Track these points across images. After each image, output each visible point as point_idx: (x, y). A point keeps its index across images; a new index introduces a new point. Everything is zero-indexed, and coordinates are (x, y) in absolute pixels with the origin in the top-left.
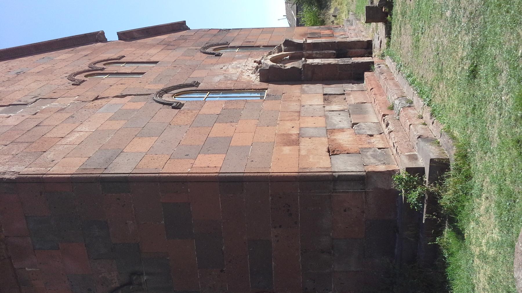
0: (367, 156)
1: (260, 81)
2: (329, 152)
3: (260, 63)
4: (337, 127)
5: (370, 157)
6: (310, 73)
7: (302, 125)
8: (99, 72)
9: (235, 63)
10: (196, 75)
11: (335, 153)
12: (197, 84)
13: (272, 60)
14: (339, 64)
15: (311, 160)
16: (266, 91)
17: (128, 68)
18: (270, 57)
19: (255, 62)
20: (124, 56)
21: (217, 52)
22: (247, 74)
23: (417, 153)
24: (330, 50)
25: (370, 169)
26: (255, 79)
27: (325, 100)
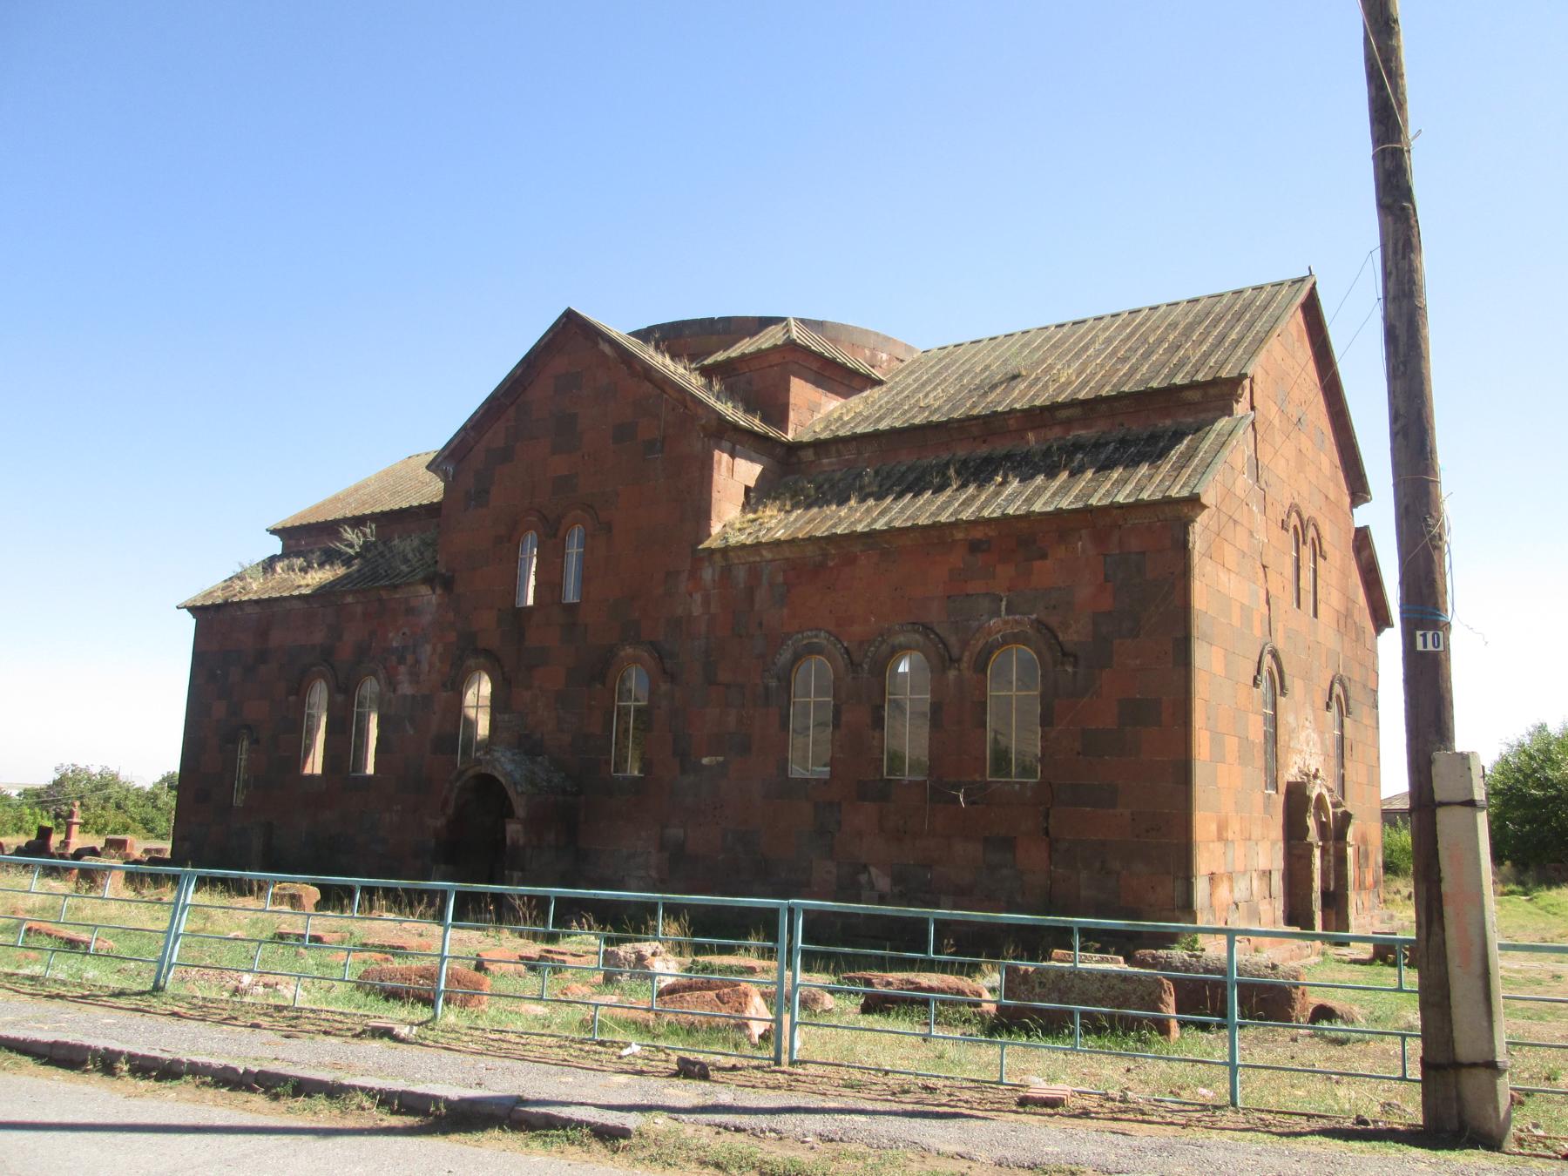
2: (1212, 874)
3: (1315, 777)
4: (1234, 885)
7: (1236, 843)
8: (1301, 539)
9: (1314, 736)
10: (1295, 684)
12: (1283, 694)
13: (1320, 797)
16: (1274, 792)
17: (1306, 576)
18: (1325, 791)
19: (1317, 770)
20: (1325, 559)
21: (1334, 704)
22: (1298, 760)
24: (1335, 883)
26: (1291, 774)
27: (1264, 872)
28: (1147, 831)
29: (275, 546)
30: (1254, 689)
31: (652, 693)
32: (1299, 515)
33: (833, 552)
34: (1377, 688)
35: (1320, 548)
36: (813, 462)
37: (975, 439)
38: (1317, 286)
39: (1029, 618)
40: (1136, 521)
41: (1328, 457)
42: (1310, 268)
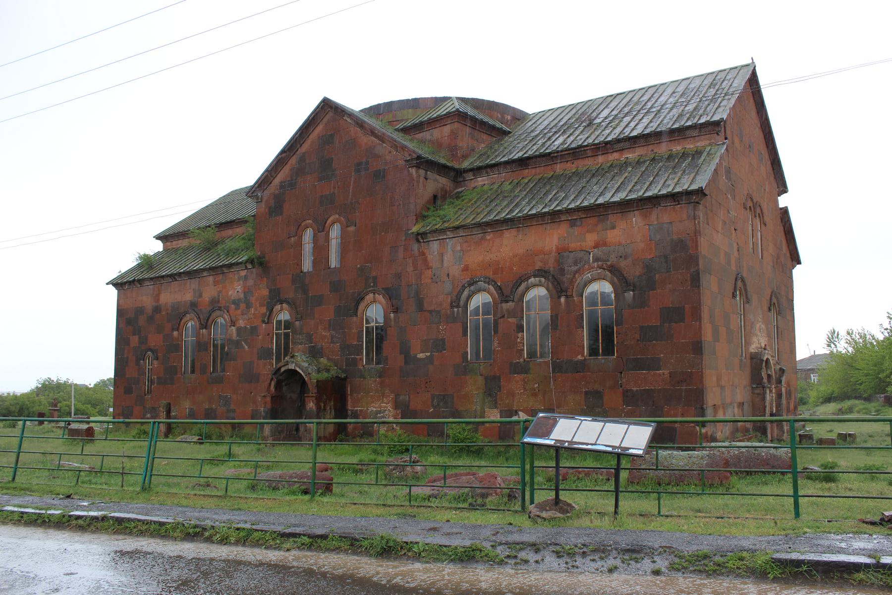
7: (726, 388)
9: (763, 326)
10: (754, 298)
13: (767, 359)
19: (765, 345)
20: (765, 225)
27: (740, 403)
28: (679, 383)
29: (159, 246)
30: (733, 300)
31: (386, 317)
32: (752, 200)
33: (489, 231)
36: (471, 180)
37: (567, 162)
38: (756, 68)
39: (606, 264)
41: (765, 168)
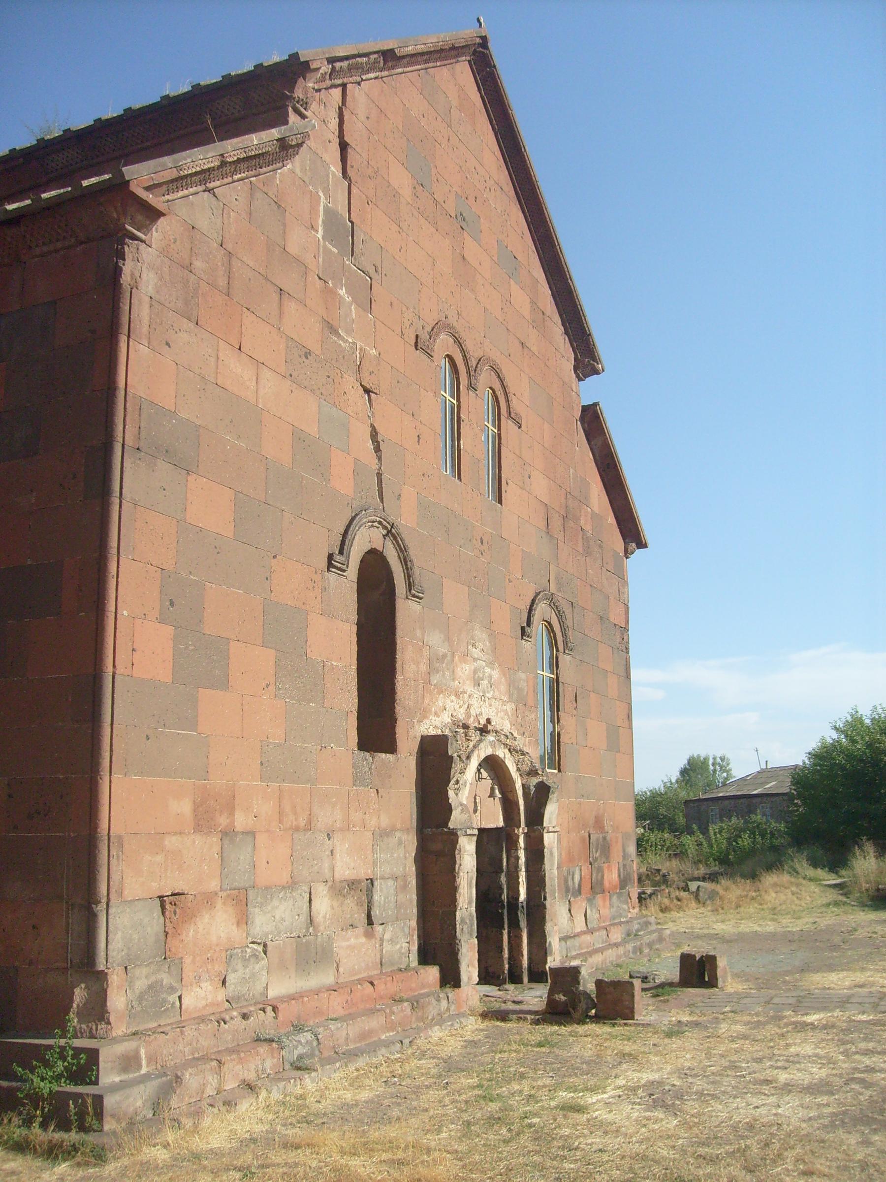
0: (159, 971)
1: (422, 736)
2: (173, 895)
4: (255, 911)
5: (153, 979)
6: (436, 846)
7: (261, 839)
9: (496, 674)
11: (168, 906)
14: (456, 911)
15: (147, 857)
19: (489, 721)
20: (520, 428)
21: (538, 629)
23: (144, 1070)
25: (115, 979)
27: (353, 884)
30: (332, 577)
34: (627, 622)
35: (509, 406)
40: (45, 249)
42: (478, 20)
